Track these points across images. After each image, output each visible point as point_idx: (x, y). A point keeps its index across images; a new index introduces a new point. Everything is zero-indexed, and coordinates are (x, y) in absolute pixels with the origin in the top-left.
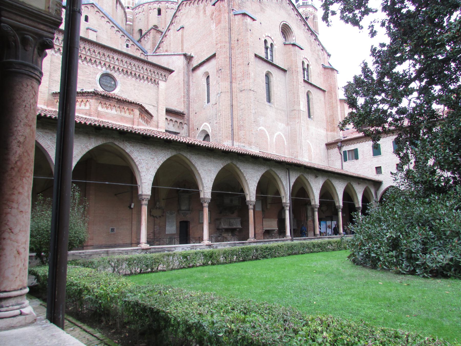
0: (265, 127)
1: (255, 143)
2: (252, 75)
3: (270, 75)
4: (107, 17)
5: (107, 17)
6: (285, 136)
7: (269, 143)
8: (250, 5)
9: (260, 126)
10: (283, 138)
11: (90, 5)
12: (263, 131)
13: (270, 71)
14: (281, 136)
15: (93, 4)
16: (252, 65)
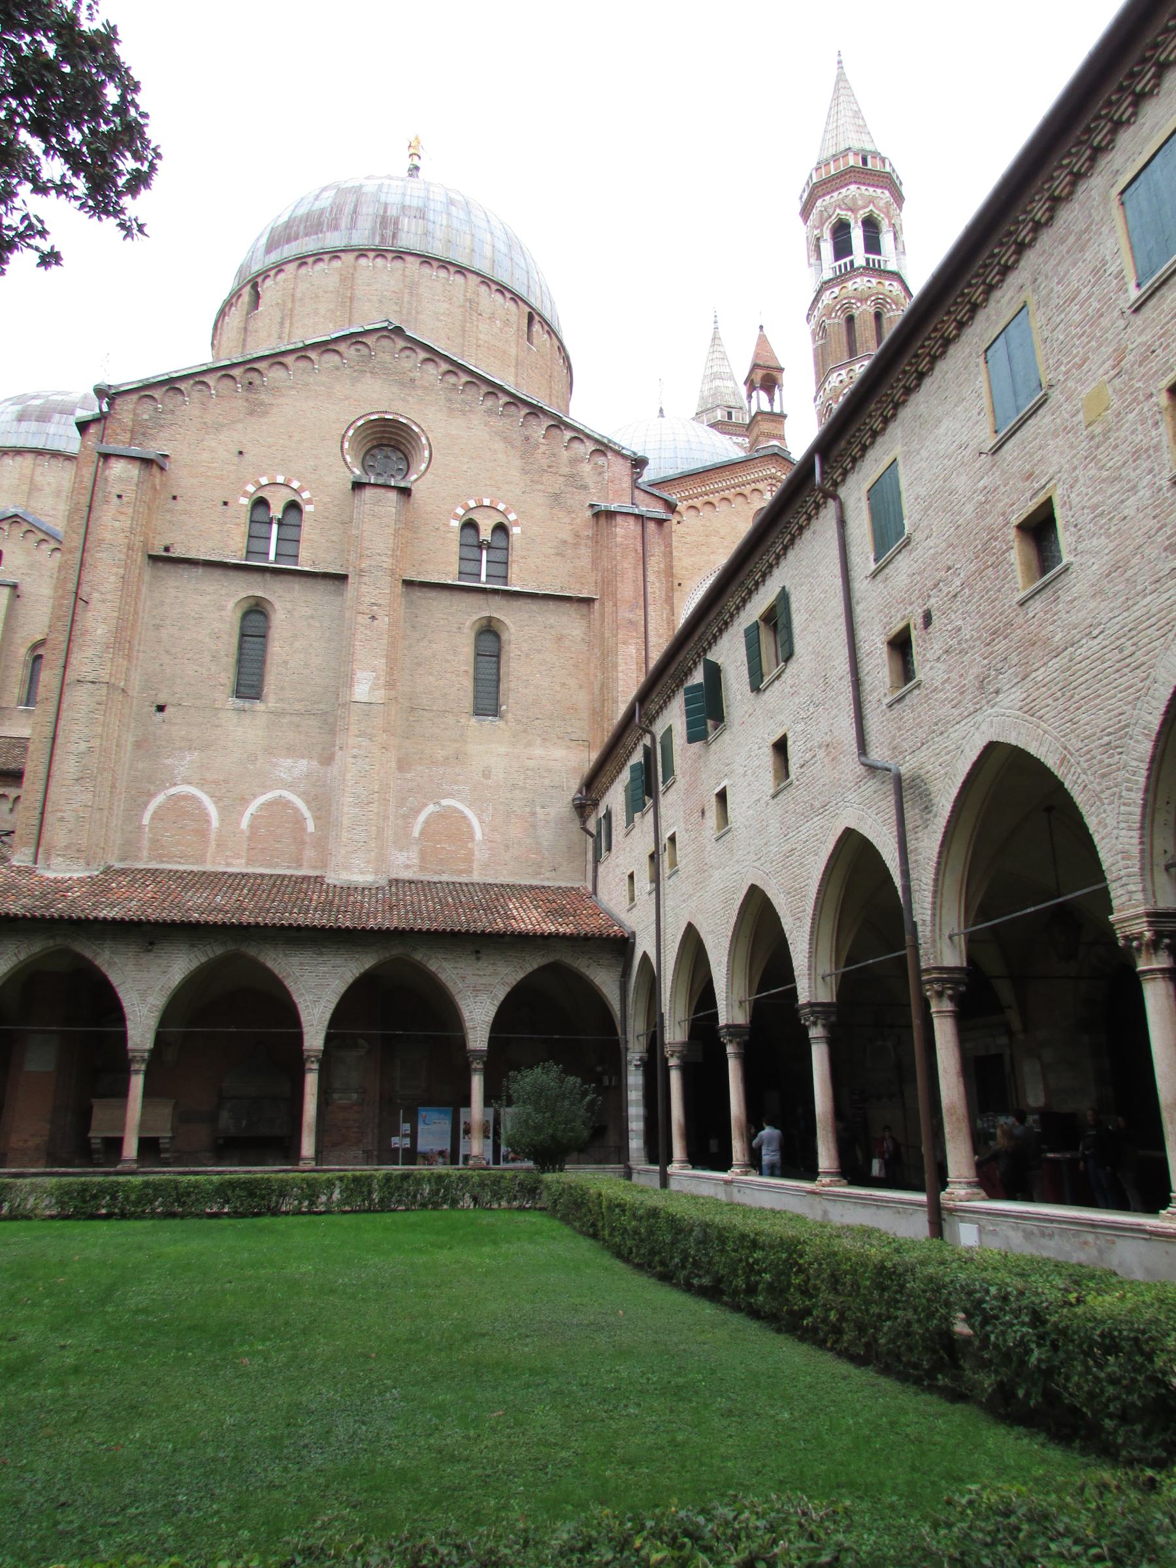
0: (202, 784)
1: (67, 847)
2: (99, 632)
3: (269, 608)
4: (54, 538)
5: (54, 538)
6: (307, 802)
7: (213, 836)
8: (197, 413)
9: (175, 785)
10: (296, 810)
11: (10, 521)
12: (193, 798)
13: (259, 594)
14: (289, 802)
15: (16, 516)
16: (103, 601)
